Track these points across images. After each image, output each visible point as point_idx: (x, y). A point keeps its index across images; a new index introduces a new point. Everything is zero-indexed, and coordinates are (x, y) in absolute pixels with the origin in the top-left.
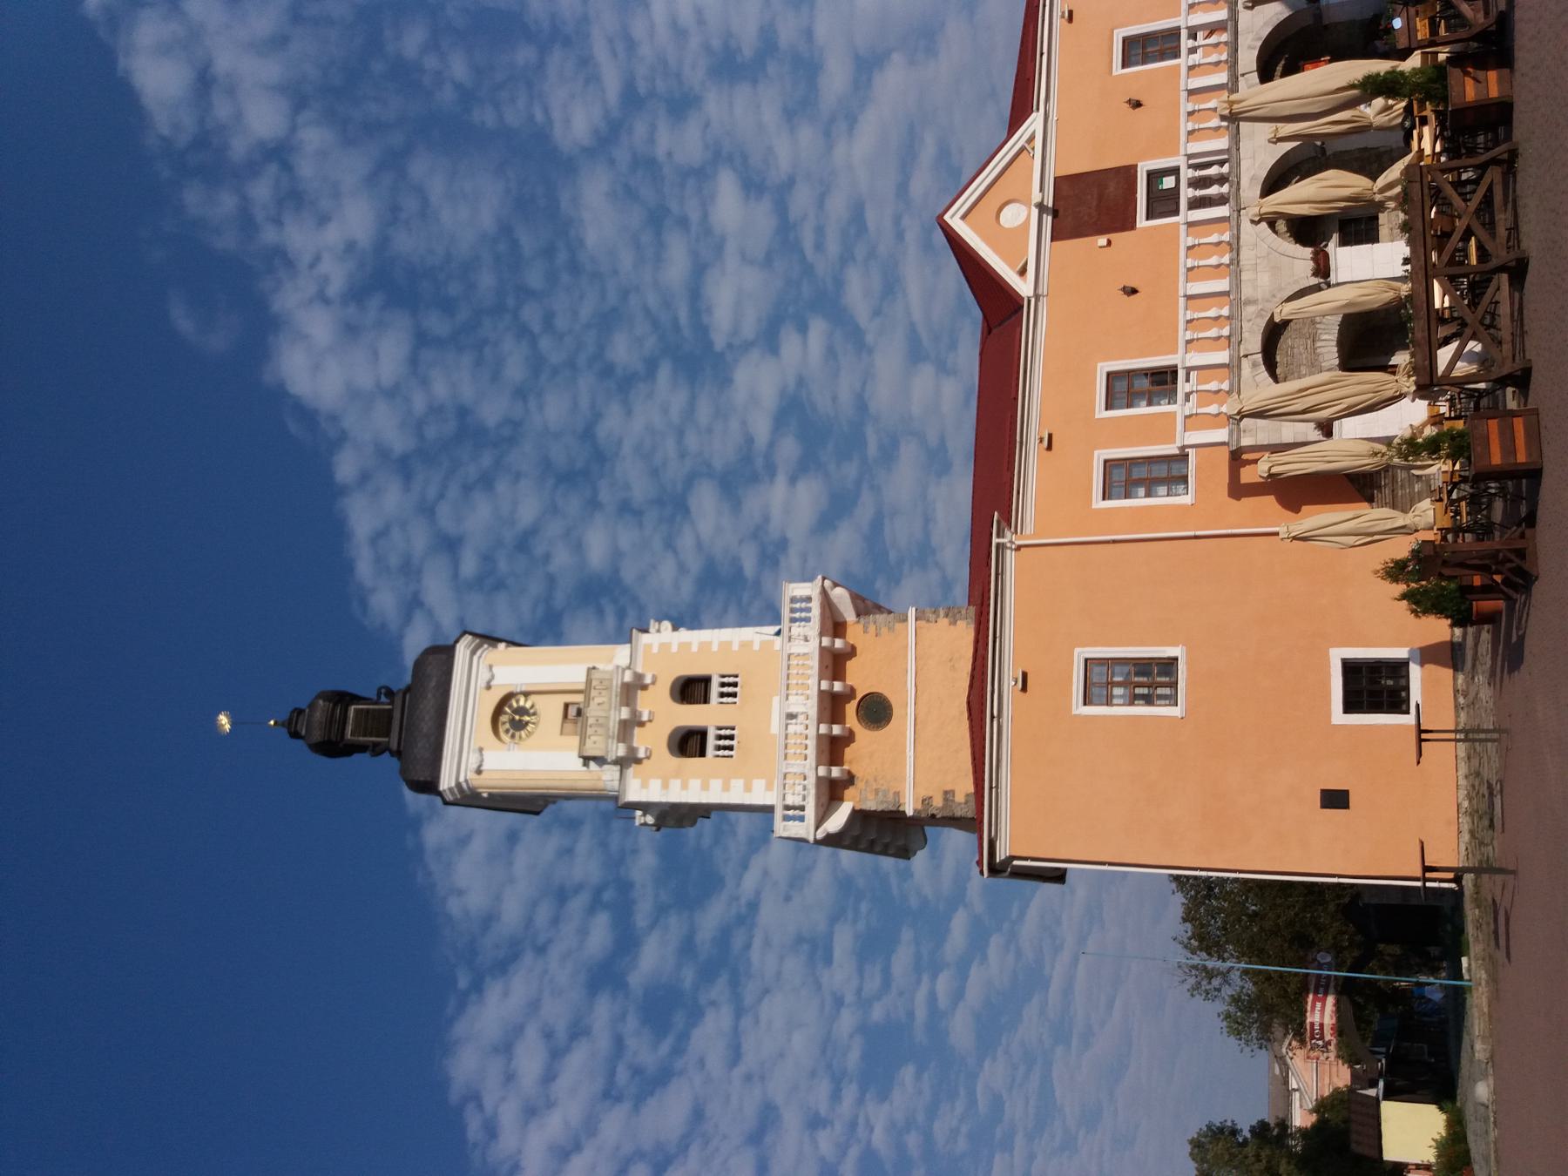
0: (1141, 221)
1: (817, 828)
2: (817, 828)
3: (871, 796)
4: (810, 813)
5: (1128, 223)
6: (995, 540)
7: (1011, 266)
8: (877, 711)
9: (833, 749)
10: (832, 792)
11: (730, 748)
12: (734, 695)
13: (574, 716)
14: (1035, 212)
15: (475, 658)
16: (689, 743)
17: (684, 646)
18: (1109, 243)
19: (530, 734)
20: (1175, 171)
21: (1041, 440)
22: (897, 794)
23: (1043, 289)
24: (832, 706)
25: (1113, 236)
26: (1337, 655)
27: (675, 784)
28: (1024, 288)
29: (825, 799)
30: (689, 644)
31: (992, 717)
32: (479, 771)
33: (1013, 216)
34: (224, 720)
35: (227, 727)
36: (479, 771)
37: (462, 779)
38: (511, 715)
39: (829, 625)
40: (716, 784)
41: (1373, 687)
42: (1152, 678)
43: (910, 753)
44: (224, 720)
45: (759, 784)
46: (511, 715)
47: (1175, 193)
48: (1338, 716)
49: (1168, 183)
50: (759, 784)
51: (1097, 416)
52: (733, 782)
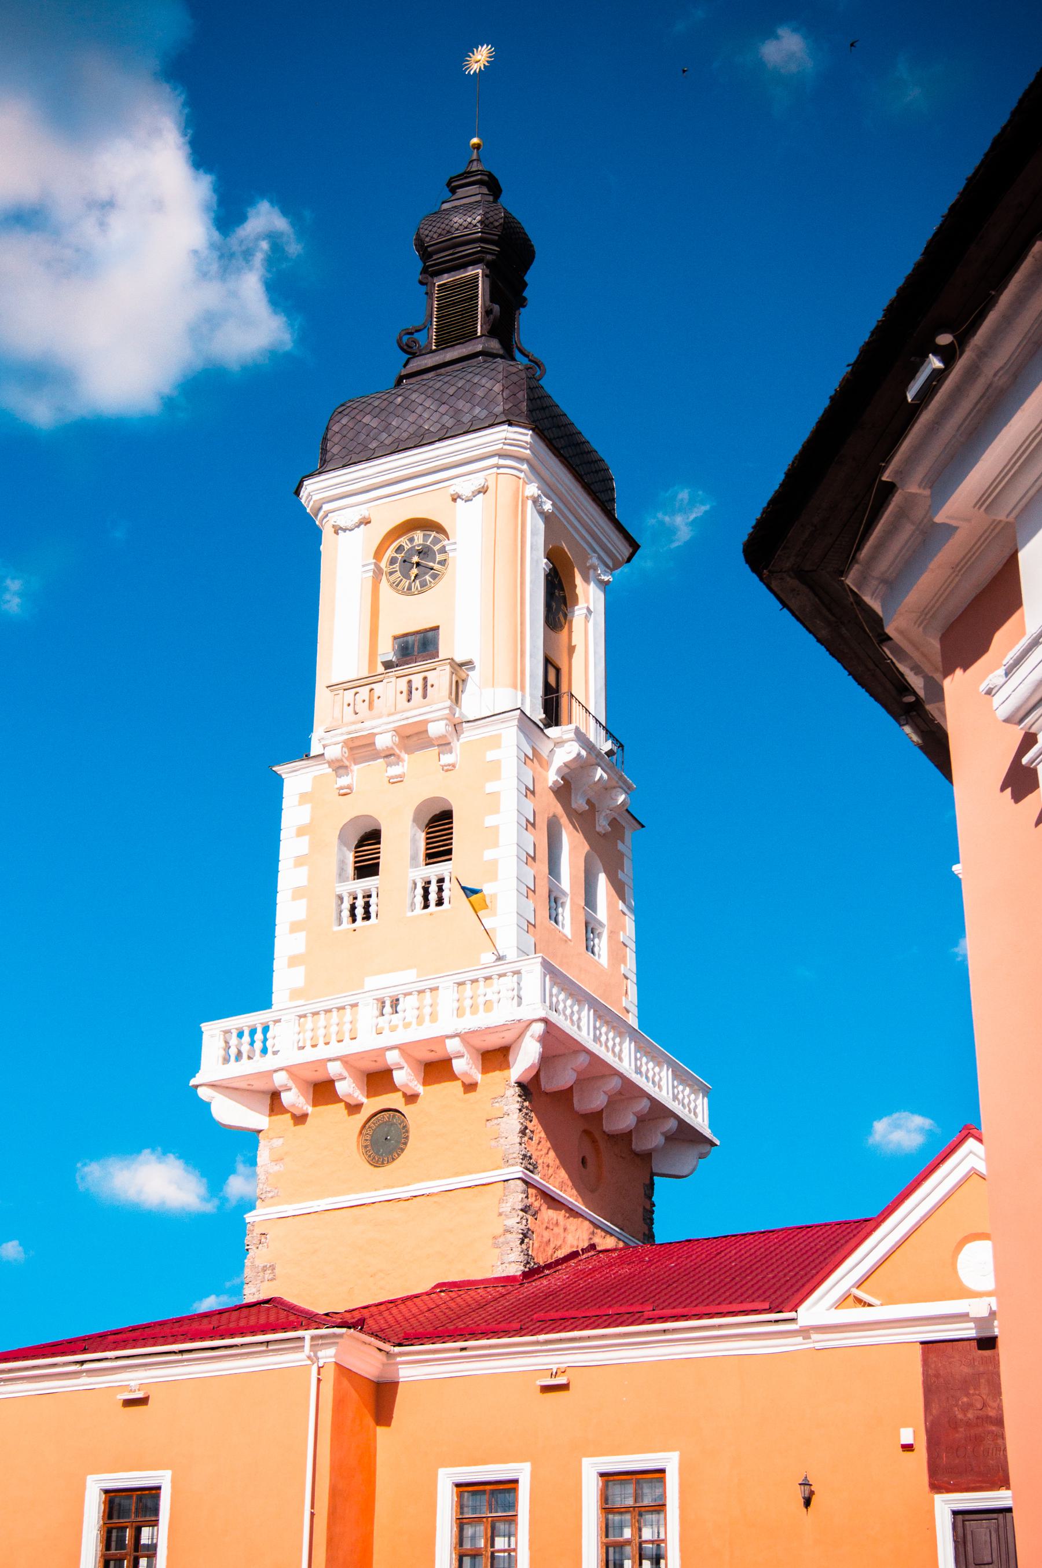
0: (944, 1506)
1: (212, 1086)
2: (212, 1086)
5: (941, 1480)
6: (307, 1334)
8: (385, 1141)
11: (353, 917)
13: (418, 647)
15: (495, 460)
16: (366, 852)
17: (493, 803)
18: (908, 1448)
19: (395, 586)
23: (819, 1340)
30: (496, 810)
31: (82, 1363)
32: (337, 530)
34: (480, 57)
35: (475, 68)
36: (337, 530)
37: (326, 507)
38: (415, 553)
44: (480, 57)
51: (586, 1462)
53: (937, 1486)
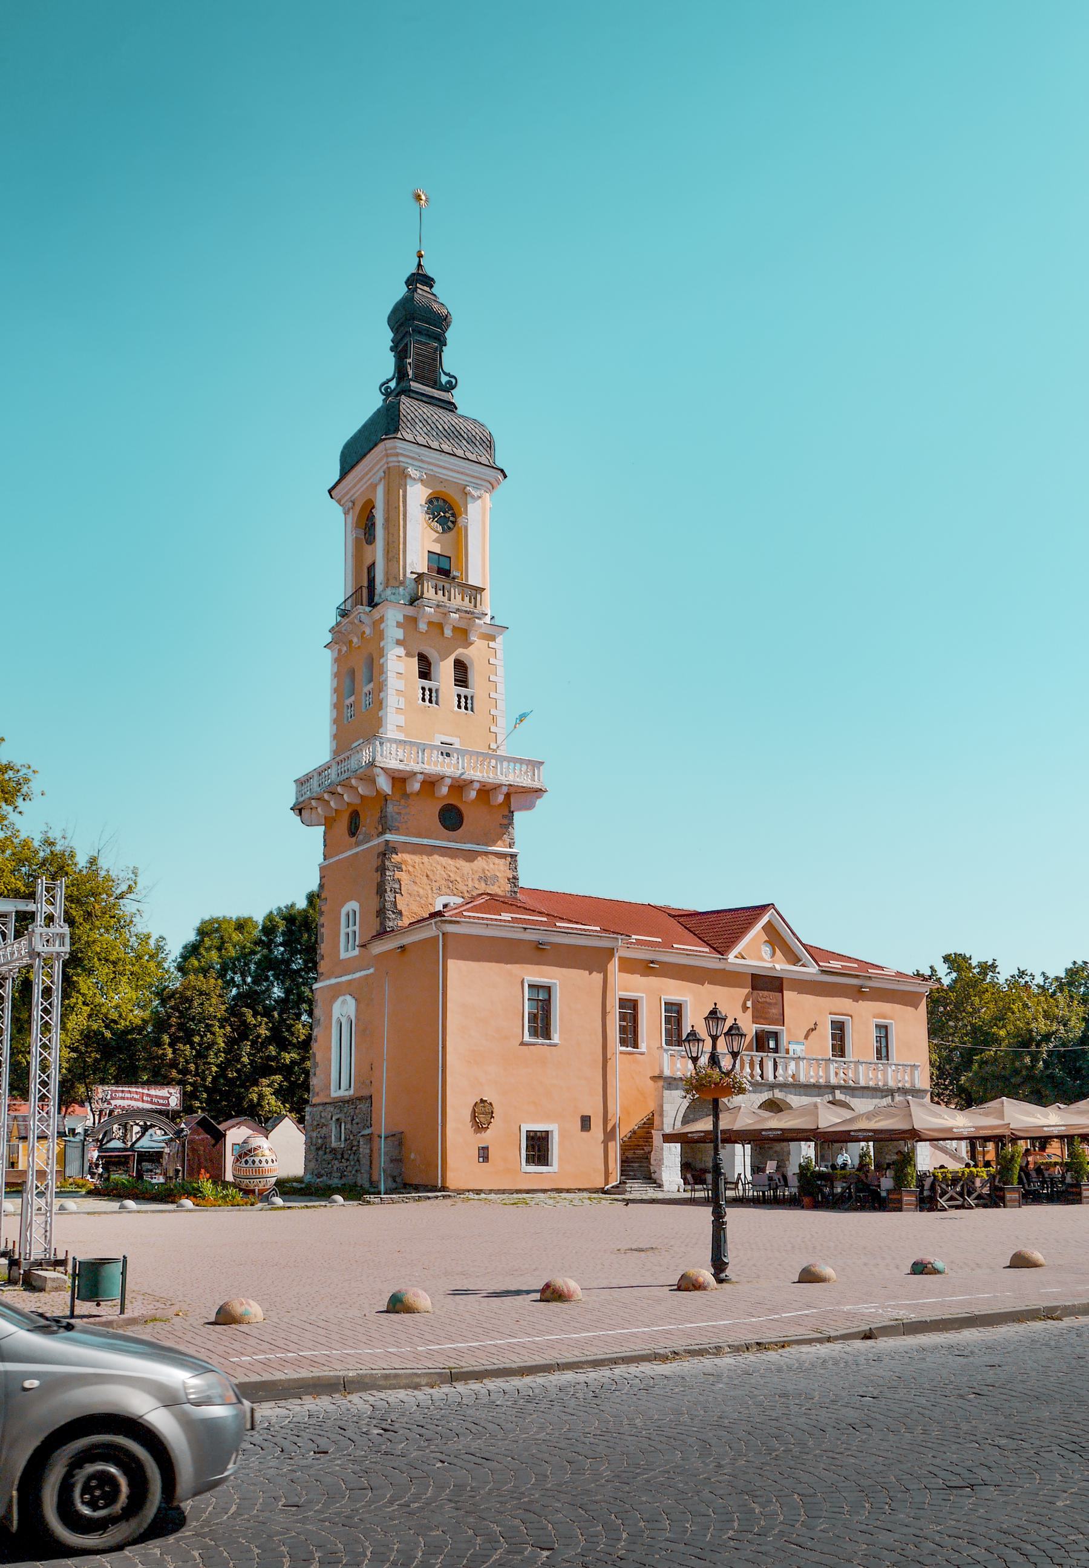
3: (396, 809)
4: (393, 764)
7: (743, 949)
9: (431, 783)
10: (399, 780)
12: (459, 707)
14: (770, 965)
20: (776, 1050)
21: (652, 962)
22: (398, 829)
24: (459, 786)
25: (749, 1012)
26: (552, 1127)
27: (401, 651)
28: (731, 957)
29: (396, 775)
33: (766, 950)
39: (512, 790)
40: (400, 685)
41: (538, 1148)
42: (541, 1023)
43: (425, 841)
45: (401, 720)
46: (445, 512)
47: (769, 1050)
48: (525, 1127)
49: (772, 1044)
50: (401, 720)
52: (402, 700)
53: (753, 1022)
